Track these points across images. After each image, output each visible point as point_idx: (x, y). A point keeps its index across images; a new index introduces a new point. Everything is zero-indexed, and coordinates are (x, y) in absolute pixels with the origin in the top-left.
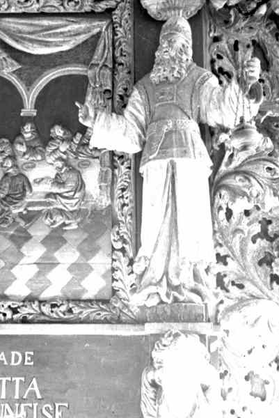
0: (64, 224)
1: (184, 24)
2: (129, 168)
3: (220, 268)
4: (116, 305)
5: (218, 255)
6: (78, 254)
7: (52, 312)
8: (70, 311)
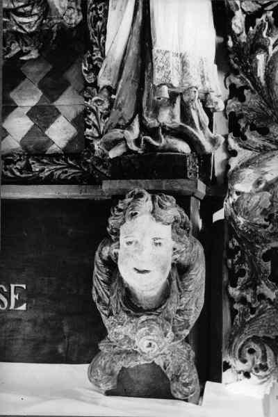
0: (21, 53)
3: (234, 104)
4: (89, 161)
6: (40, 93)
7: (6, 169)
8: (28, 168)
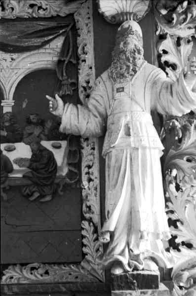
1: (136, 27)
2: (93, 149)
5: (170, 220)
